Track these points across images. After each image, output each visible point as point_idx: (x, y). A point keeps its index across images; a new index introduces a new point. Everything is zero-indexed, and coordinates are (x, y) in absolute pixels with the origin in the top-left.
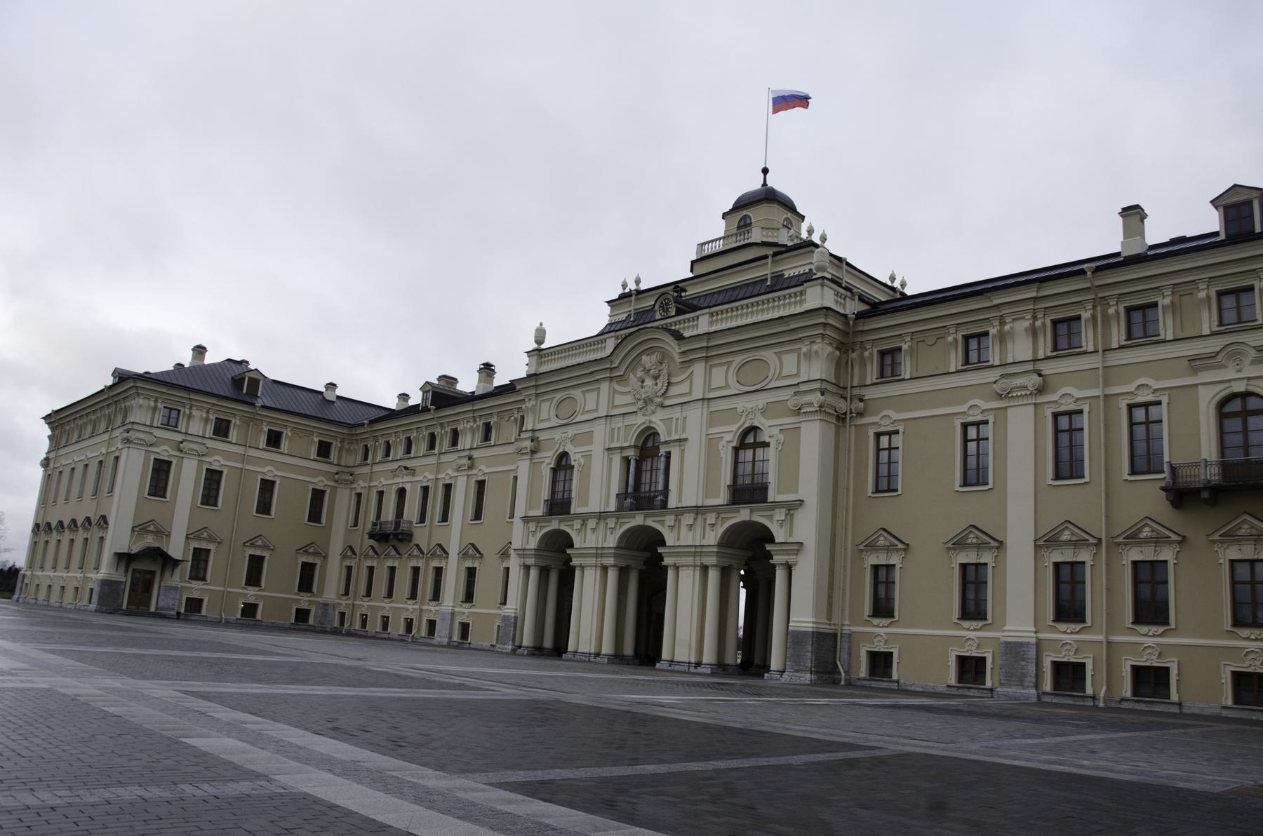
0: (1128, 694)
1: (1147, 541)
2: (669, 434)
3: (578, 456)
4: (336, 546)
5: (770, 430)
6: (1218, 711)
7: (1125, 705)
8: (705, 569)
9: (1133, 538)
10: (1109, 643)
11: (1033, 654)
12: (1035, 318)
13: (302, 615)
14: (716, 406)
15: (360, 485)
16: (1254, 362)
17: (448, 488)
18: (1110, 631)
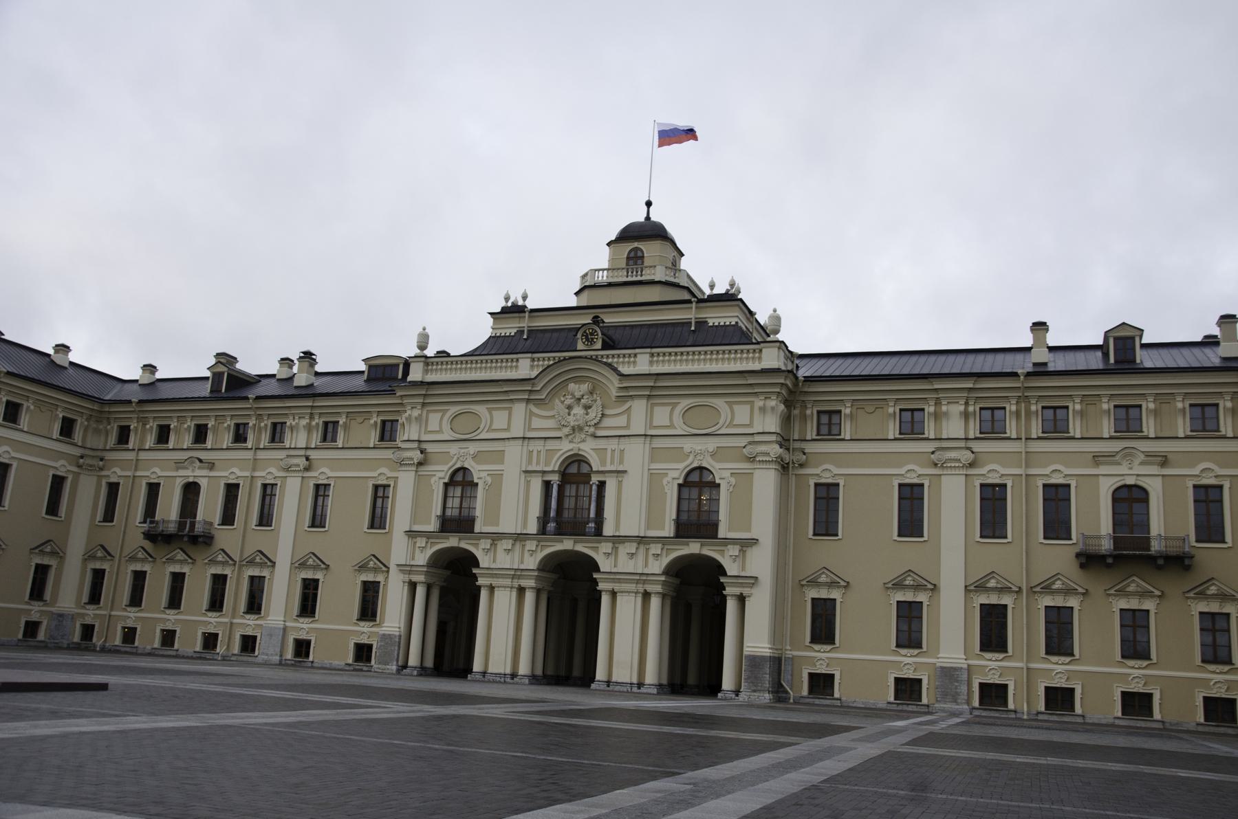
0: (1043, 709)
1: (1058, 591)
2: (603, 463)
3: (483, 474)
4: (284, 558)
5: (722, 472)
6: (1111, 721)
7: (1041, 717)
8: (521, 590)
9: (1047, 588)
10: (1028, 669)
11: (965, 676)
12: (967, 404)
13: (31, 628)
14: (658, 443)
15: (116, 474)
16: (1142, 463)
17: (268, 491)
18: (1028, 661)
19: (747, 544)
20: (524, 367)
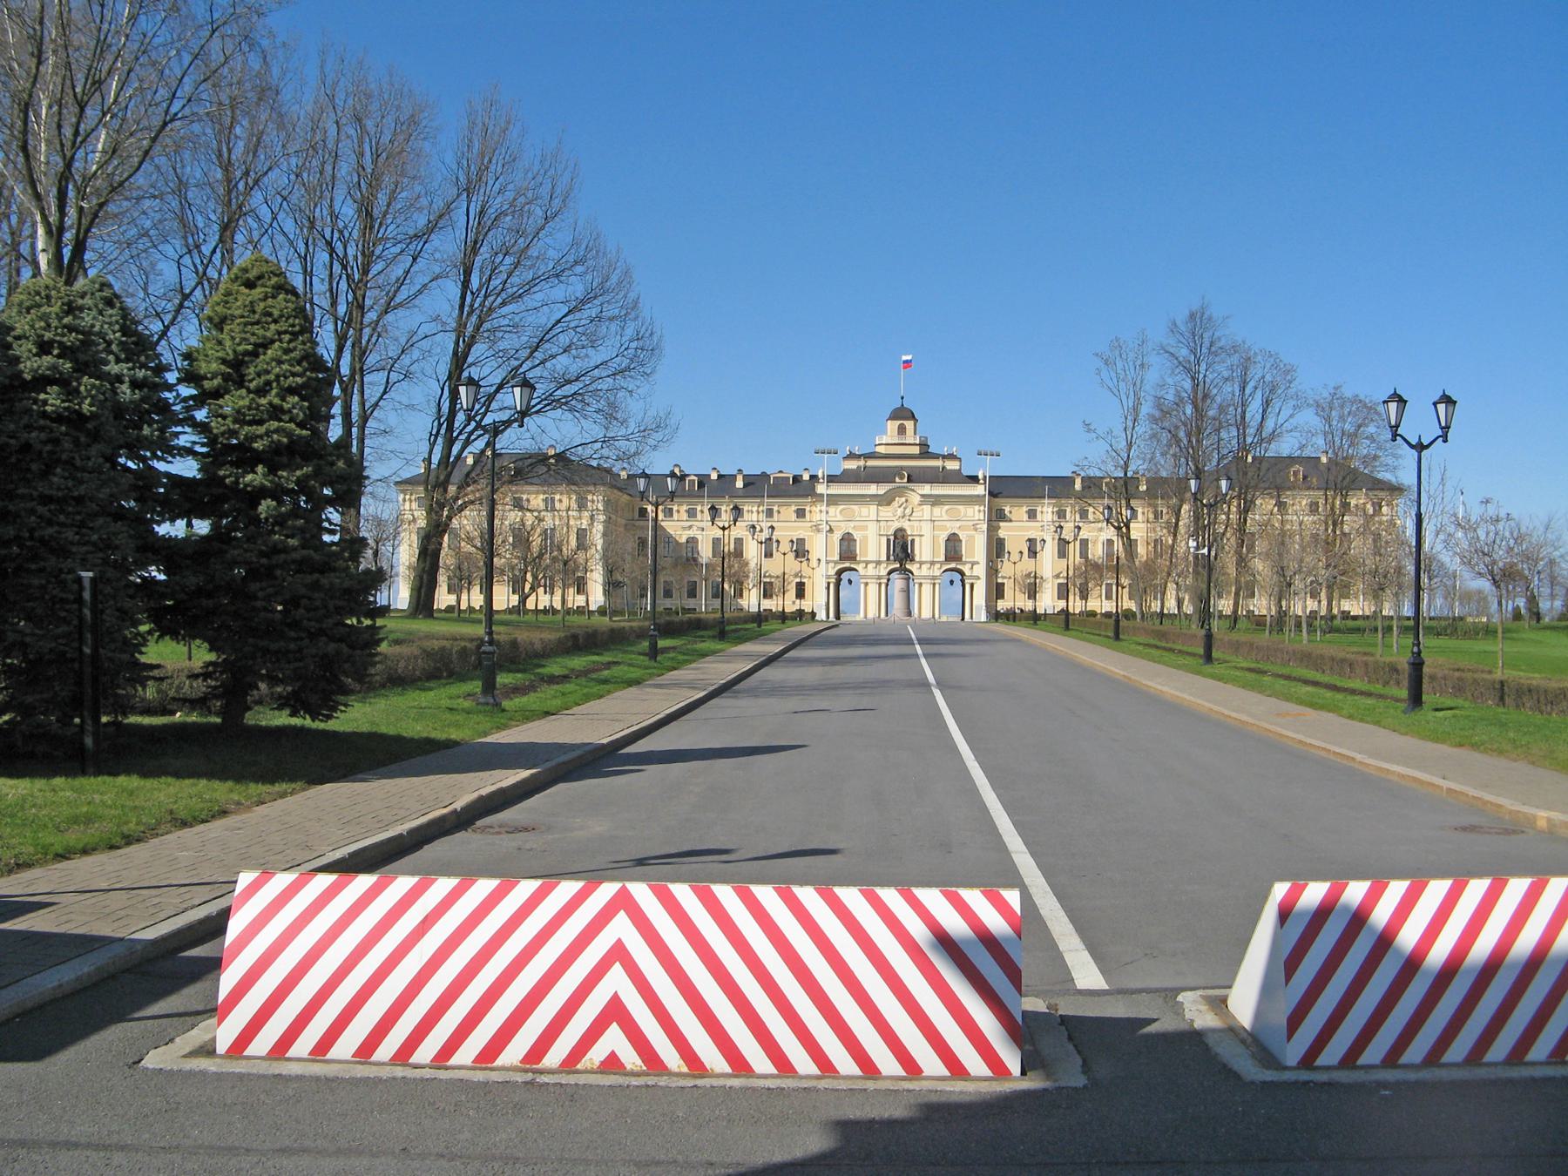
19: (973, 564)
20: (873, 489)
